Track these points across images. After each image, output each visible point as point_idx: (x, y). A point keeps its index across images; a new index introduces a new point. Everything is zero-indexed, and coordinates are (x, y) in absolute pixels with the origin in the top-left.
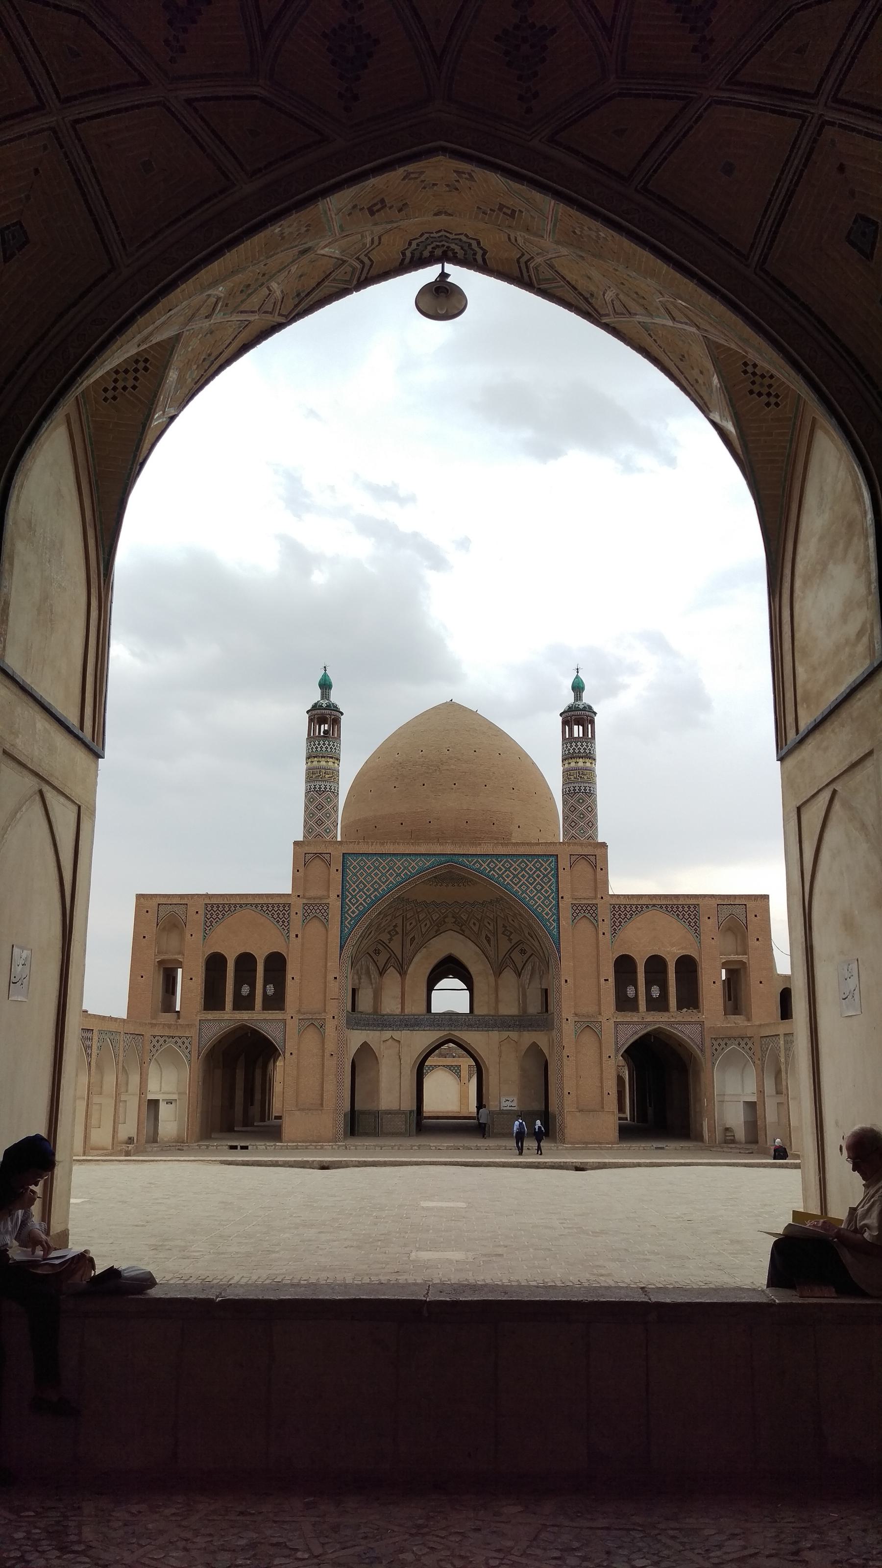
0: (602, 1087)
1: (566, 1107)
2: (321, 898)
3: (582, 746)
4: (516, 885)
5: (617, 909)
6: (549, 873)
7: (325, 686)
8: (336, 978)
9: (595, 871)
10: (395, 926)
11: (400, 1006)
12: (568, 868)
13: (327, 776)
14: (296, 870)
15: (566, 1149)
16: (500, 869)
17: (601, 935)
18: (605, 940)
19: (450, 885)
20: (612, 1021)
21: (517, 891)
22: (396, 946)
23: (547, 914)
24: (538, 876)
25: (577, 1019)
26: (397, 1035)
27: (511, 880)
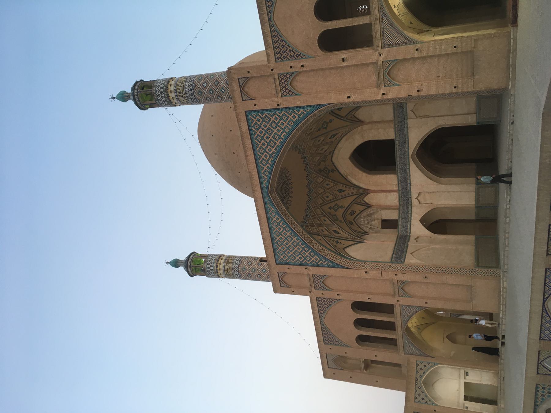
0: (448, 55)
1: (469, 90)
2: (310, 279)
3: (159, 95)
4: (275, 143)
5: (279, 55)
6: (260, 117)
7: (176, 263)
8: (366, 272)
9: (252, 78)
10: (330, 208)
11: (392, 193)
12: (254, 102)
13: (229, 270)
14: (293, 293)
15: (514, 86)
16: (266, 156)
17: (305, 68)
18: (309, 65)
19: (290, 181)
20: (381, 51)
21: (280, 142)
22: (346, 202)
23: (294, 117)
24: (265, 126)
25: (382, 86)
26: (414, 195)
27: (273, 147)
